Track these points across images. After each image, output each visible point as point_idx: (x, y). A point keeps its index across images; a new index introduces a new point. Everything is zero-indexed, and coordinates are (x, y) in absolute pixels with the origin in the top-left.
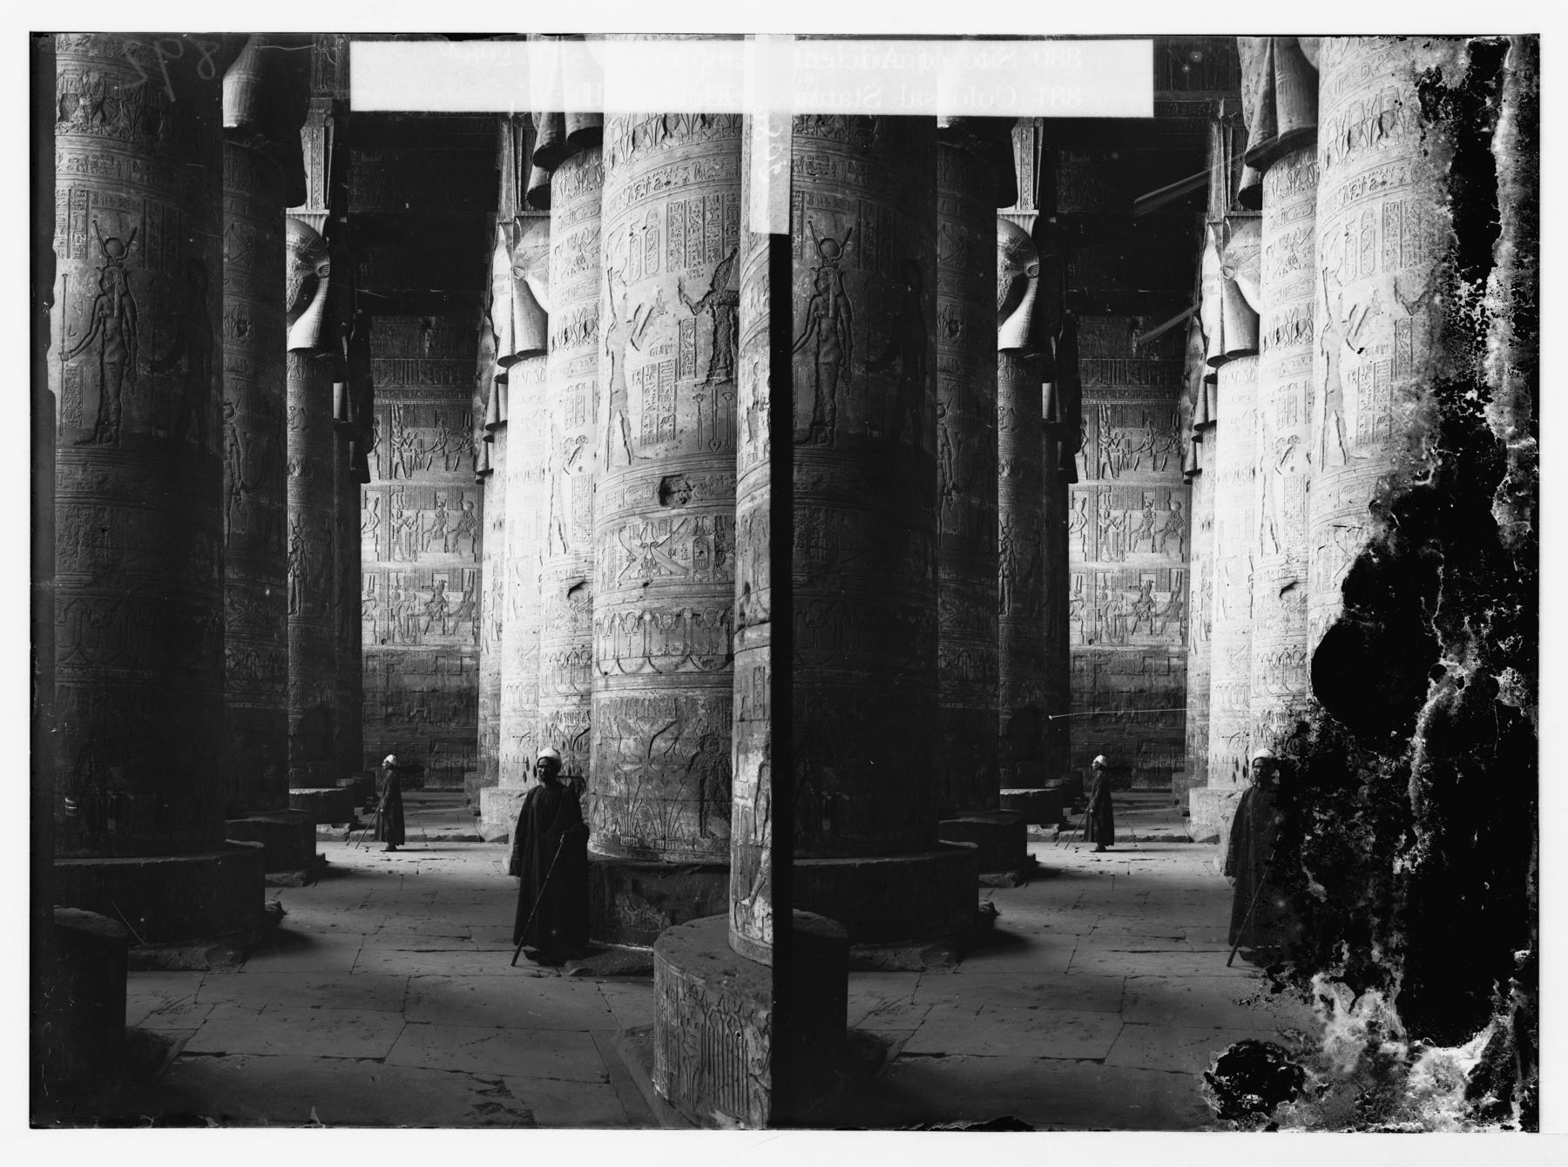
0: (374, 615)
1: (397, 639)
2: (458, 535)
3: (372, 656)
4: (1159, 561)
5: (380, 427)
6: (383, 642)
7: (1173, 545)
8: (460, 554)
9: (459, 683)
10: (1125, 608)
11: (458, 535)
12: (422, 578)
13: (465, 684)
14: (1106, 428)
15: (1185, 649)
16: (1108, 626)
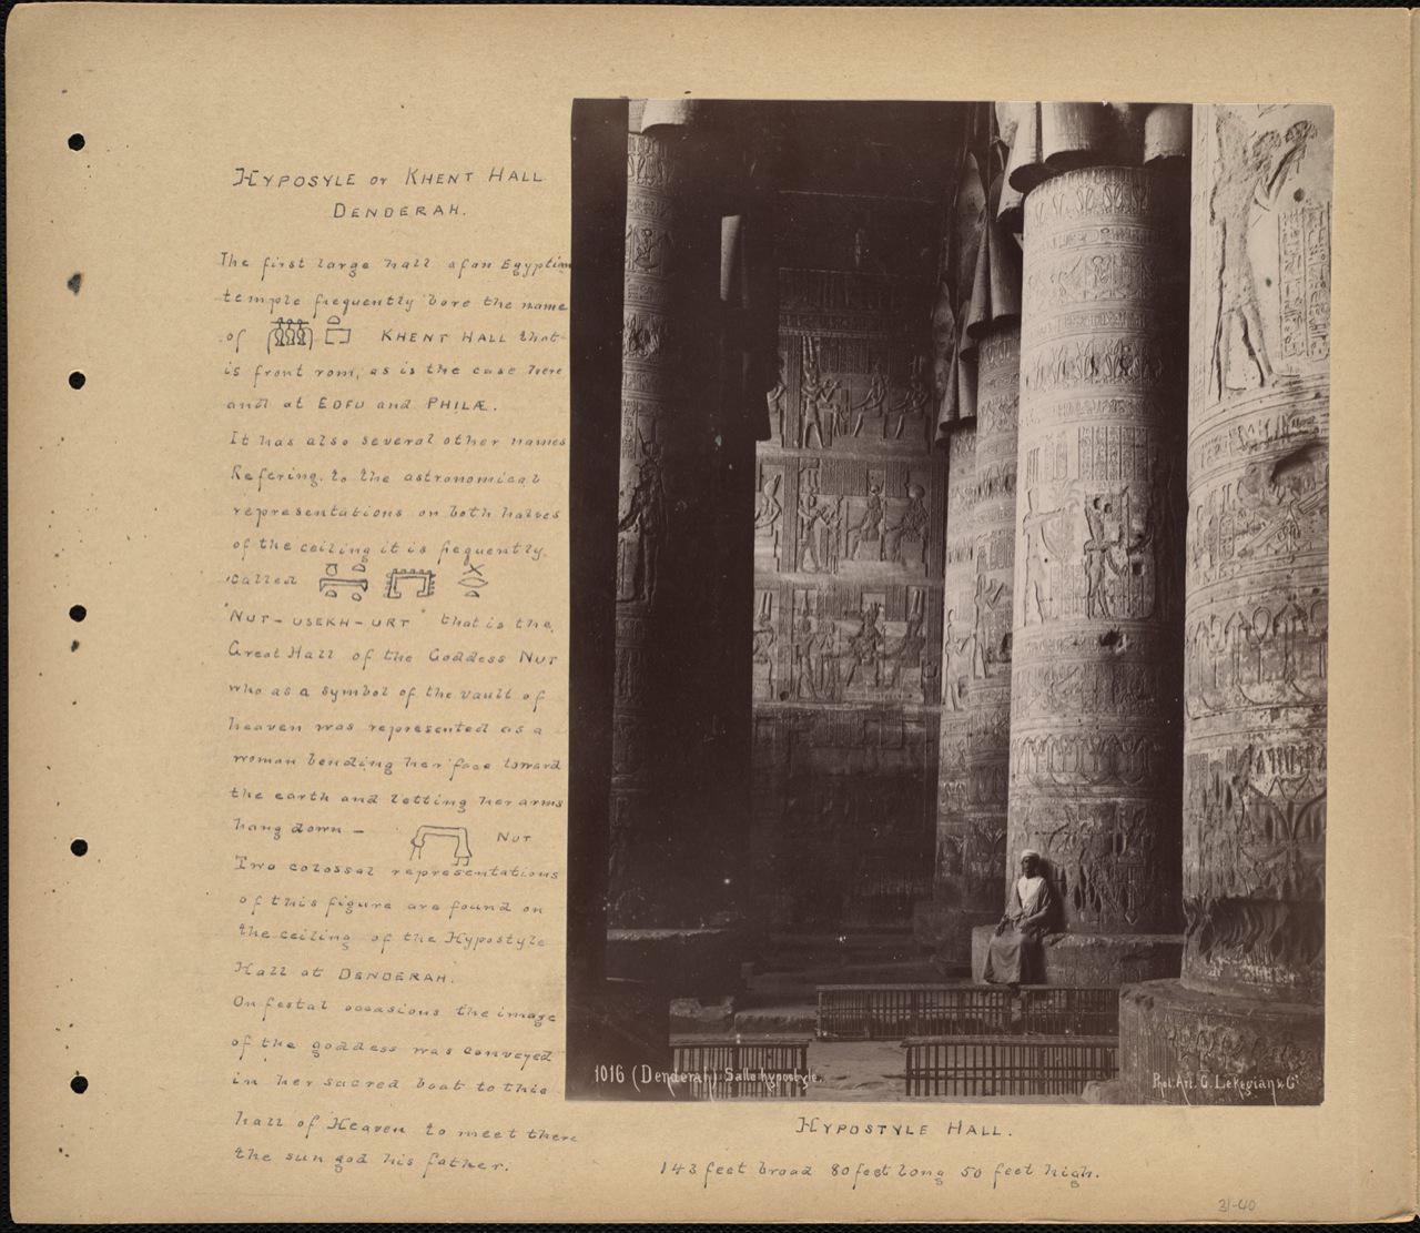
0: (769, 653)
1: (805, 692)
2: (901, 534)
3: (766, 718)
4: (891, 574)
5: (785, 369)
6: (783, 696)
7: (911, 550)
8: (904, 564)
9: (899, 762)
10: (837, 644)
11: (901, 534)
12: (845, 600)
13: (909, 764)
14: (813, 372)
15: (934, 709)
16: (811, 672)
